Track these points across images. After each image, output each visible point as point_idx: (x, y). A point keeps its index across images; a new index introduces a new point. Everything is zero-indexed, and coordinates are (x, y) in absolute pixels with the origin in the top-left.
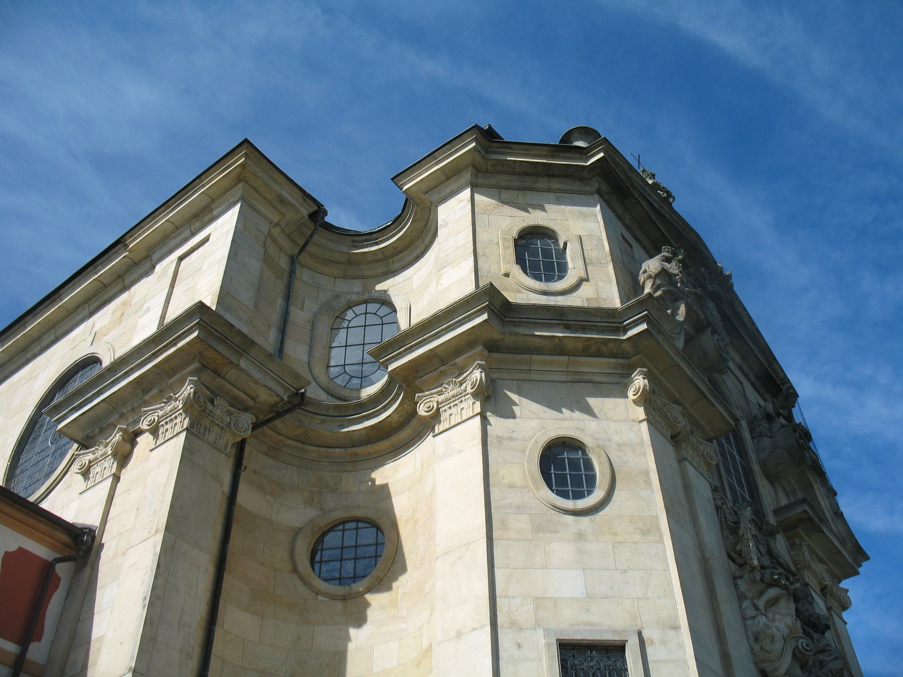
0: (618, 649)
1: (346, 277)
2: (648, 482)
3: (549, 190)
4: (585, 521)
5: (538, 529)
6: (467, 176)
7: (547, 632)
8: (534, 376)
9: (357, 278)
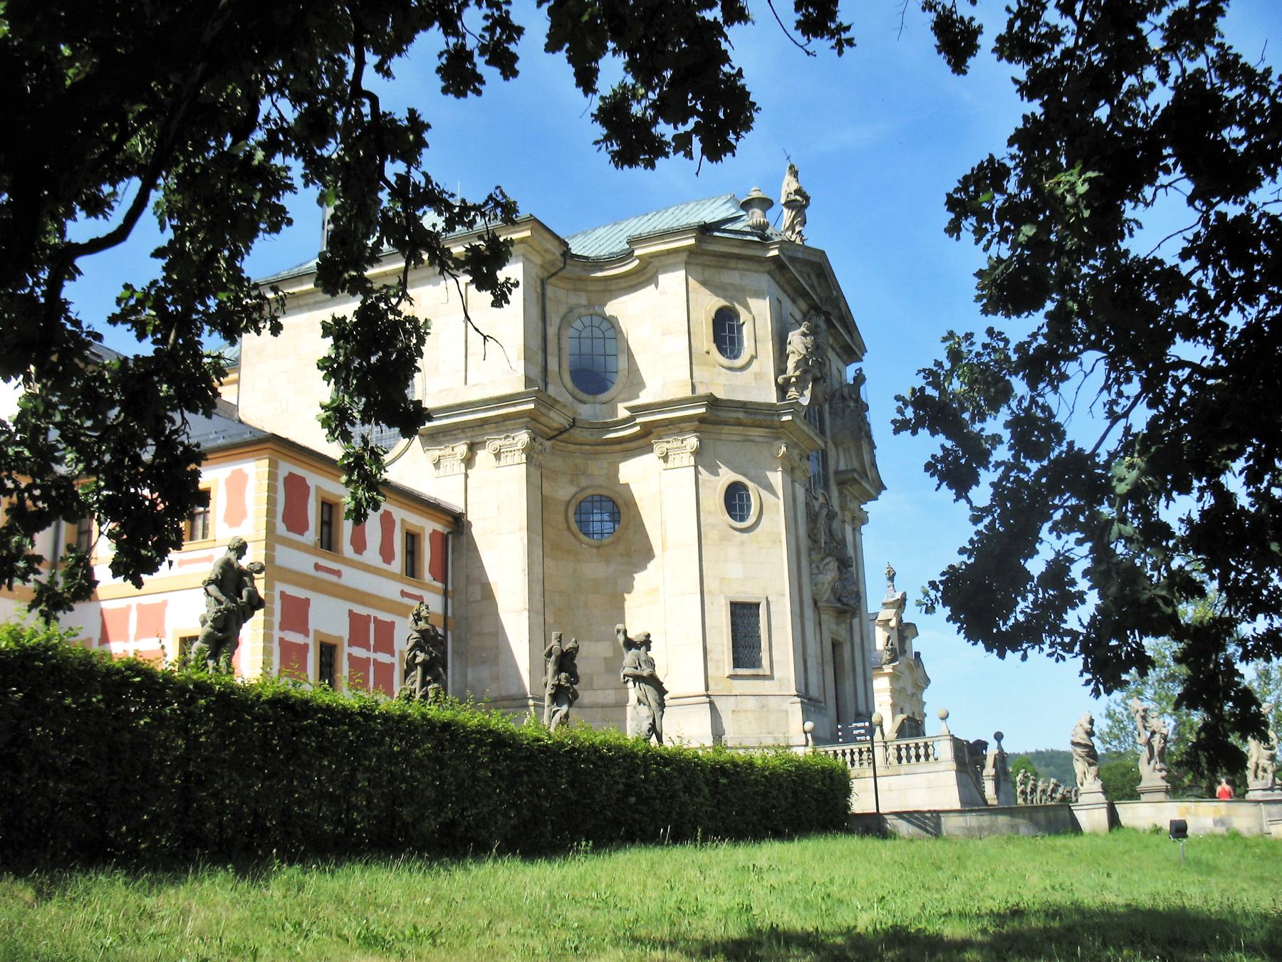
0: (758, 605)
1: (575, 290)
2: (778, 511)
3: (735, 269)
4: (745, 535)
5: (722, 539)
6: (684, 257)
7: (726, 597)
8: (723, 437)
9: (581, 290)
